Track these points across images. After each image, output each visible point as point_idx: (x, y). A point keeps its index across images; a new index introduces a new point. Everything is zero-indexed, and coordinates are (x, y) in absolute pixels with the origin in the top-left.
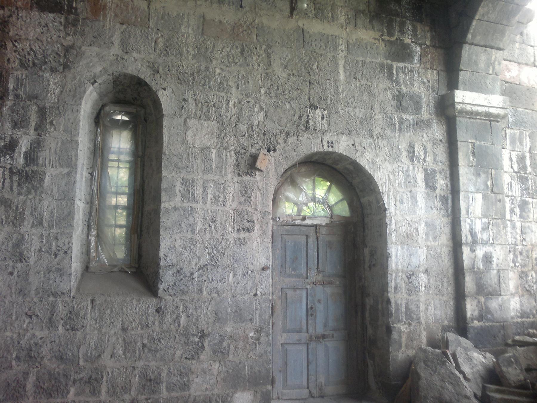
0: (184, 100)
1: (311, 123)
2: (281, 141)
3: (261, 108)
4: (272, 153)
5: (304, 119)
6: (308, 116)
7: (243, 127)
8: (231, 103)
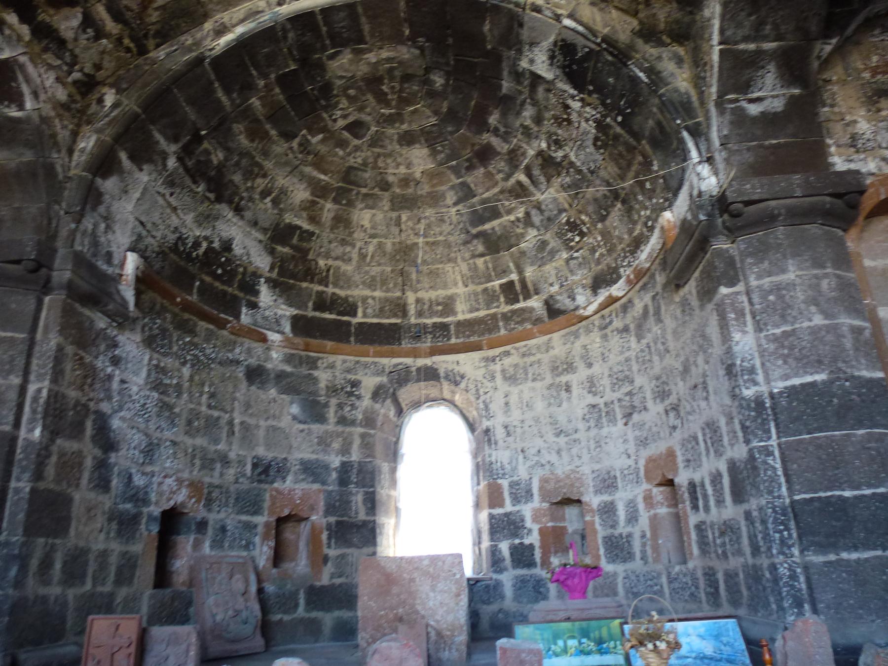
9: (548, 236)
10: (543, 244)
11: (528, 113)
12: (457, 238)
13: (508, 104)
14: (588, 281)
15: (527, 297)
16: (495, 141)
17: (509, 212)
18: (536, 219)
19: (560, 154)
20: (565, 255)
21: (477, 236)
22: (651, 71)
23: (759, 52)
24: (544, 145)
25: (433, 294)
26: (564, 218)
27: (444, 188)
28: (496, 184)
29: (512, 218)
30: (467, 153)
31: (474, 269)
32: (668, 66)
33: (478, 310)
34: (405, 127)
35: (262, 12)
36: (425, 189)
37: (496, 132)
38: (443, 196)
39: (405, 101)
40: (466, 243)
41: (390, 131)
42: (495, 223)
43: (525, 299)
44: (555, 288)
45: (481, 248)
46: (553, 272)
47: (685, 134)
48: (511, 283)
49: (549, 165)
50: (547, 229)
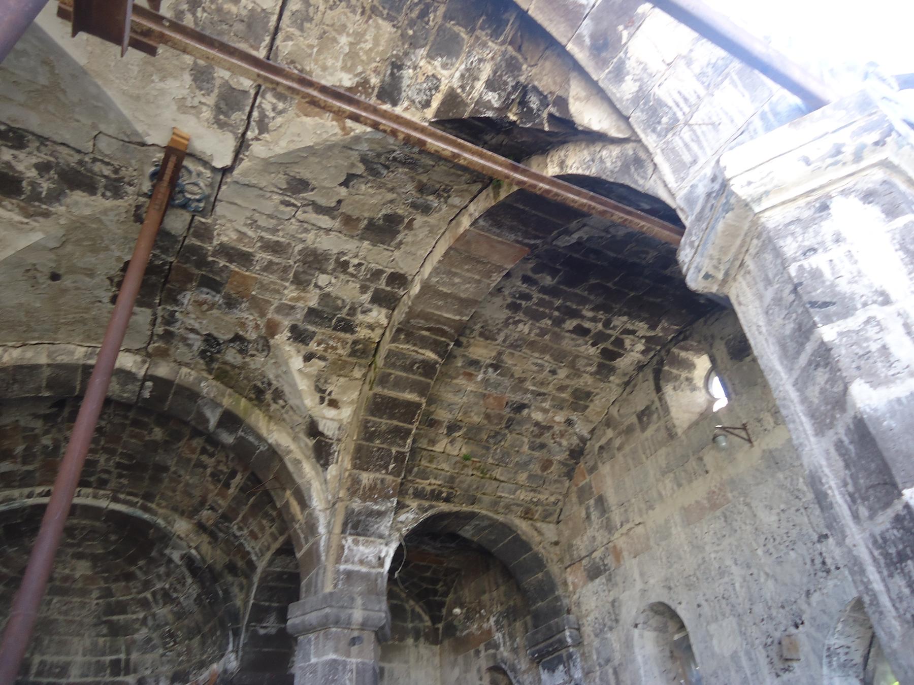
0: (699, 606)
1: (829, 561)
2: (804, 607)
3: (767, 574)
4: (801, 627)
5: (818, 561)
6: (821, 554)
7: (759, 609)
8: (737, 585)
9: (154, 635)
10: (149, 640)
11: (162, 570)
12: (90, 620)
13: (152, 561)
14: (170, 674)
15: (127, 673)
16: (138, 573)
17: (134, 613)
18: (150, 622)
19: (175, 595)
20: (161, 651)
21: (105, 622)
22: (226, 592)
23: (269, 607)
24: (167, 586)
25: (56, 659)
26: (167, 628)
27: (92, 587)
28: (131, 594)
29: (134, 617)
30: (117, 573)
31: (95, 644)
32: (235, 590)
33: (87, 676)
34: (80, 550)
35: (15, 500)
36: (80, 585)
37: (140, 568)
38: (91, 592)
39: (84, 539)
40: (95, 625)
41: (70, 551)
42: (122, 617)
43: (125, 675)
44: (148, 672)
45: (105, 631)
46: (150, 661)
47: (230, 633)
48: (119, 661)
49: (167, 597)
50: (155, 630)
